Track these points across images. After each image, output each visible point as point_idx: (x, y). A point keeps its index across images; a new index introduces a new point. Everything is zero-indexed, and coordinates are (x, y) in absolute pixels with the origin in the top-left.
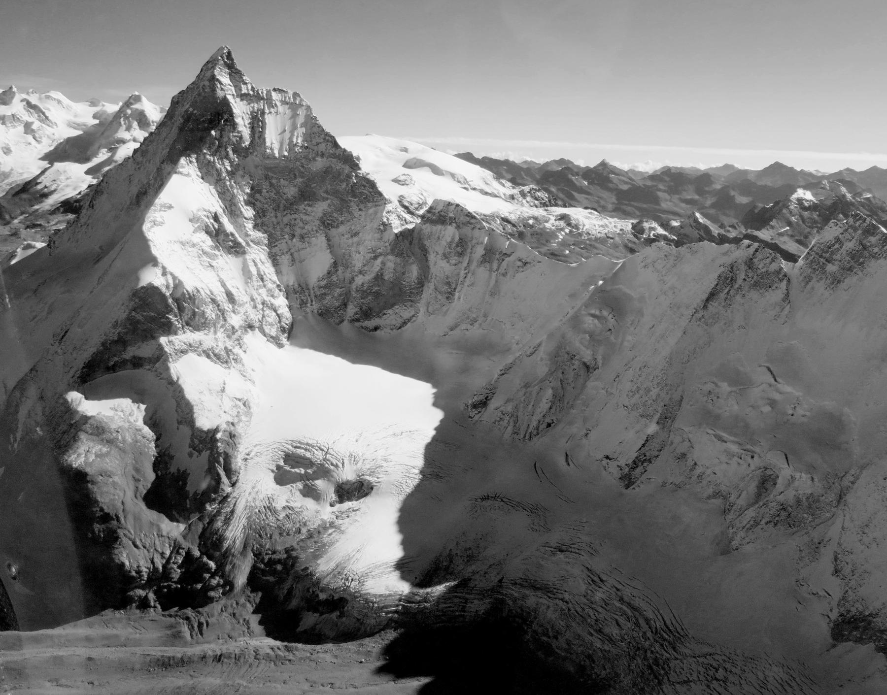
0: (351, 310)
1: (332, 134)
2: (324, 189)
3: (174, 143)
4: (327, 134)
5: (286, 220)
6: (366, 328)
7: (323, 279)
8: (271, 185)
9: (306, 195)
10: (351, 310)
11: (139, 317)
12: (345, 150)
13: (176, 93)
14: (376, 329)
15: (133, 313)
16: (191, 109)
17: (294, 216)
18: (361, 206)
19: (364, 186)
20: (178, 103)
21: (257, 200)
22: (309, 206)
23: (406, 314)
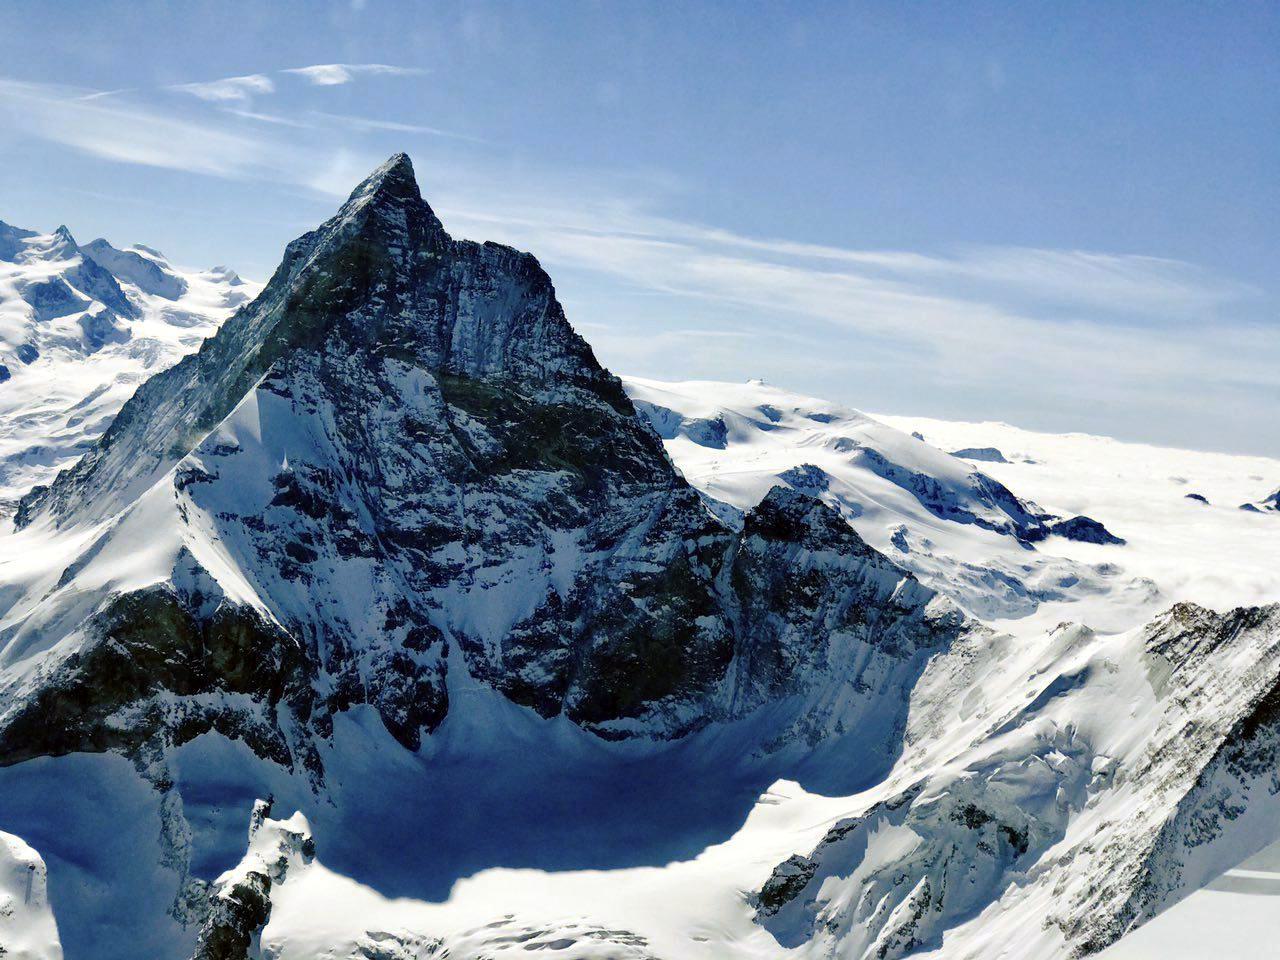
0: (575, 694)
1: (587, 339)
2: (555, 446)
3: (274, 332)
4: (578, 340)
5: (471, 500)
6: (602, 733)
7: (524, 626)
8: (453, 429)
9: (517, 456)
10: (575, 694)
11: (122, 650)
12: (606, 373)
13: (297, 235)
14: (622, 735)
15: (112, 641)
16: (316, 269)
17: (487, 496)
18: (625, 488)
19: (637, 449)
20: (298, 255)
21: (415, 455)
22: (523, 478)
23: (686, 712)
